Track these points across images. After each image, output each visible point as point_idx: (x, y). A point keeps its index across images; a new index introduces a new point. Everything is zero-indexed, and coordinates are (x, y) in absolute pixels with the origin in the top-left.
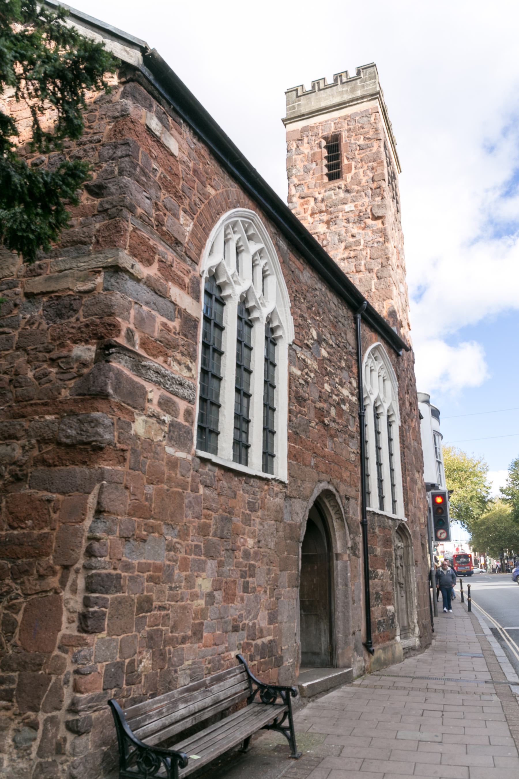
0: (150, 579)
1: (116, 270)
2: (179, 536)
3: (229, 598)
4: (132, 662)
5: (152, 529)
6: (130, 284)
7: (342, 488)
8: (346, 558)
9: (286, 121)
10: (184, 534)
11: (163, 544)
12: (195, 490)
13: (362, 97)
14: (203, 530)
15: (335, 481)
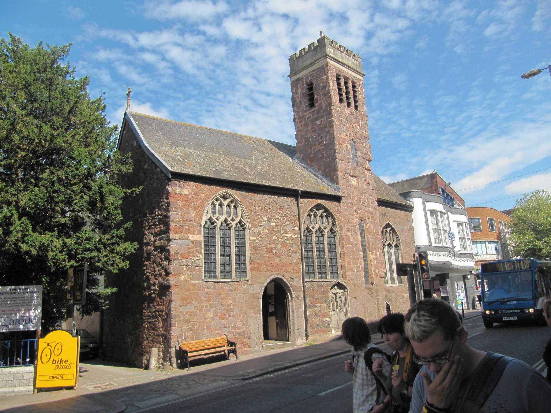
4: (185, 334)
5: (189, 303)
11: (193, 306)
13: (320, 58)
14: (208, 301)
15: (281, 273)
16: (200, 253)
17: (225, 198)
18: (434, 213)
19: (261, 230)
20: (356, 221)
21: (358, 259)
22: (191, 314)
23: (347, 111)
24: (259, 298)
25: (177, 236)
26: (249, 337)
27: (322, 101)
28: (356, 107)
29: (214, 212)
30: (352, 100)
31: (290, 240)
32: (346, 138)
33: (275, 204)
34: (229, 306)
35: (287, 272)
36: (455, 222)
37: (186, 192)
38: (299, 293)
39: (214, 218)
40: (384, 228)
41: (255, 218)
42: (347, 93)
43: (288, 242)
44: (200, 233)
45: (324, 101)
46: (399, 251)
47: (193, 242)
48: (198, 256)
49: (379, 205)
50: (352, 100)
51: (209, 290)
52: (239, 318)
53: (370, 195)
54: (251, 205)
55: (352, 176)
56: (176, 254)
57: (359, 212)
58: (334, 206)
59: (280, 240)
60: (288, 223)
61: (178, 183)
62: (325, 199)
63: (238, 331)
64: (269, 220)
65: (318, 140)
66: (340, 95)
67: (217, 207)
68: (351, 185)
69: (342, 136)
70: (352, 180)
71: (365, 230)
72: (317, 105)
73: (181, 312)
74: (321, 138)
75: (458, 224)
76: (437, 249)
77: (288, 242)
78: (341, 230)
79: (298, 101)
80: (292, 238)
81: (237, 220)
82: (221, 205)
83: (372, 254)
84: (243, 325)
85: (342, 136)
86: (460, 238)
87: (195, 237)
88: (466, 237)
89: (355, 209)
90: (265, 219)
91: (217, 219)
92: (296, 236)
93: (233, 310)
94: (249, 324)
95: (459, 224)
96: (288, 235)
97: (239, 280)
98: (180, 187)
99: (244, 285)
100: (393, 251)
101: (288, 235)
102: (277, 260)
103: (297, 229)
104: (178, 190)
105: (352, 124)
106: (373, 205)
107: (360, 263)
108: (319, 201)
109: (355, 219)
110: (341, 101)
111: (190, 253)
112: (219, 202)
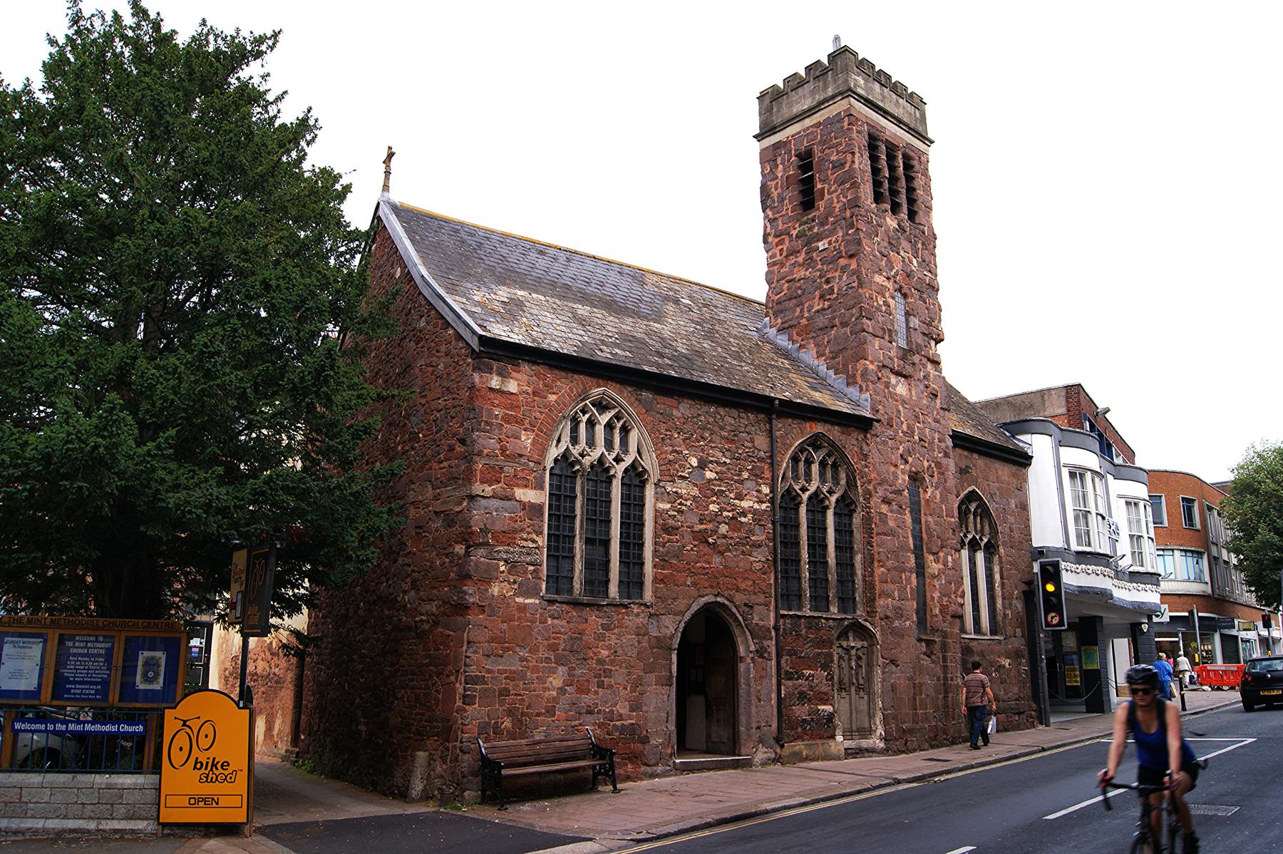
0: (506, 678)
1: (472, 498)
2: (530, 652)
3: (582, 690)
5: (508, 649)
6: (483, 502)
7: (739, 598)
8: (749, 660)
9: (759, 137)
10: (534, 650)
11: (517, 658)
12: (544, 622)
13: (833, 97)
14: (553, 648)
15: (726, 593)
16: (540, 533)
17: (602, 406)
18: (1077, 474)
19: (683, 488)
20: (903, 479)
21: (904, 571)
22: (512, 676)
23: (891, 222)
24: (670, 649)
25: (488, 490)
26: (645, 740)
27: (834, 195)
28: (912, 215)
29: (574, 440)
30: (903, 199)
31: (750, 516)
32: (886, 283)
33: (716, 429)
34: (600, 662)
35: (738, 590)
36: (1120, 497)
37: (512, 387)
38: (766, 643)
39: (575, 451)
40: (962, 503)
41: (671, 457)
42: (893, 180)
43: (743, 519)
44: (540, 487)
45: (838, 197)
46: (996, 558)
47: (524, 506)
48: (534, 541)
49: (955, 446)
50: (903, 199)
51: (556, 622)
52: (623, 693)
53: (936, 421)
54: (663, 428)
55: (898, 374)
56: (485, 531)
57: (910, 459)
58: (855, 442)
59: (725, 514)
60: (745, 475)
61: (495, 365)
62: (833, 424)
63: (618, 723)
64: (703, 465)
65: (819, 288)
66: (877, 184)
67: (583, 426)
68: (893, 396)
69: (879, 279)
70: (898, 383)
71: (923, 502)
72: (821, 204)
73: (489, 671)
74: (828, 282)
75: (1128, 503)
76: (1082, 557)
77: (743, 519)
78: (867, 500)
79: (775, 195)
80: (755, 512)
81: (628, 460)
82: (591, 424)
83: (937, 561)
84: (632, 710)
85: (879, 279)
86: (1131, 537)
87: (527, 495)
88: (1146, 536)
89: (901, 451)
90: (694, 462)
91: (582, 455)
92: (764, 506)
93: (608, 673)
94: (645, 708)
95: (1131, 503)
96: (745, 504)
97: (626, 601)
98: (499, 374)
99: (637, 615)
100: (980, 556)
101: (745, 504)
102: (717, 560)
103: (766, 490)
104: (495, 382)
105: (902, 253)
106: (943, 445)
107: (909, 580)
108: (820, 428)
109: (901, 476)
110: (878, 198)
111: (515, 531)
112: (587, 416)
